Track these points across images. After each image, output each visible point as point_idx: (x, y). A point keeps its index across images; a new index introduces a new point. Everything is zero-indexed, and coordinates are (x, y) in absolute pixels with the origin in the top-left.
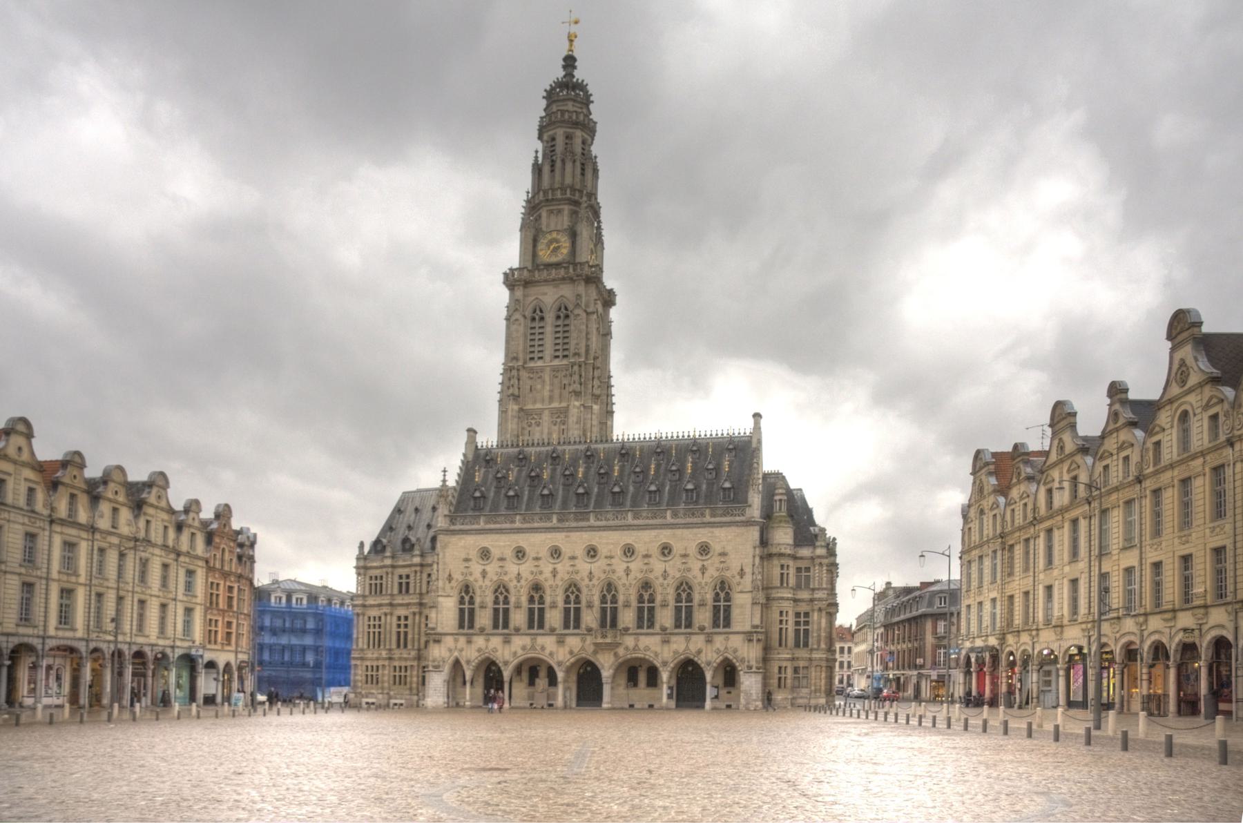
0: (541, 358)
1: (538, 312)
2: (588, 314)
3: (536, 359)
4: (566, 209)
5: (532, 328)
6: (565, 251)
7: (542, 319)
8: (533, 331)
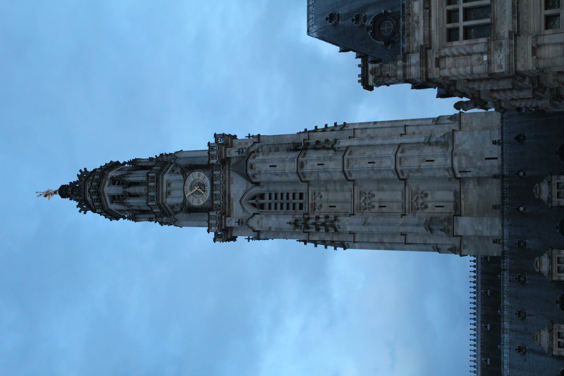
0: (301, 196)
1: (253, 201)
2: (258, 142)
3: (301, 201)
4: (167, 177)
5: (270, 208)
6: (202, 174)
7: (262, 196)
8: (273, 206)
